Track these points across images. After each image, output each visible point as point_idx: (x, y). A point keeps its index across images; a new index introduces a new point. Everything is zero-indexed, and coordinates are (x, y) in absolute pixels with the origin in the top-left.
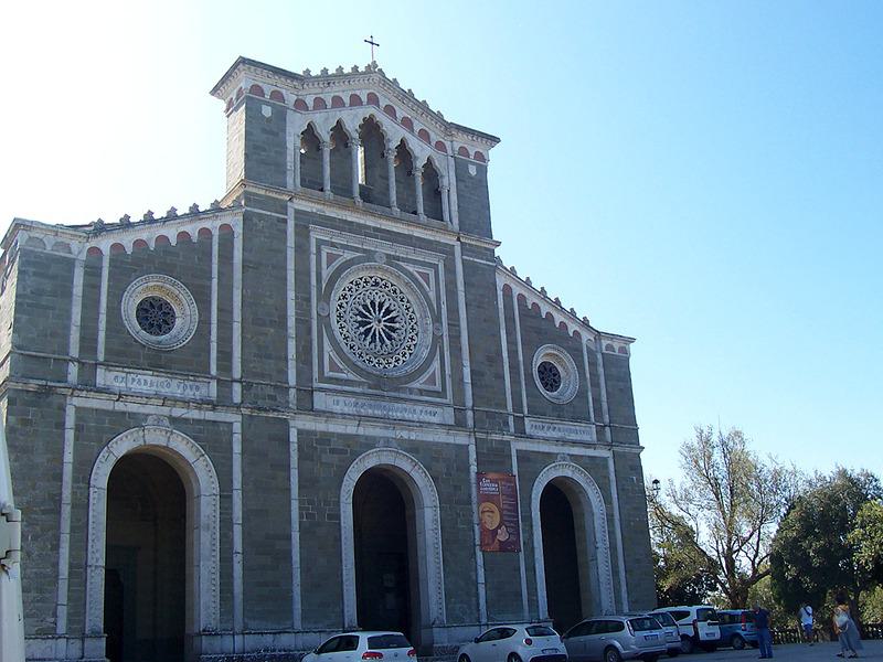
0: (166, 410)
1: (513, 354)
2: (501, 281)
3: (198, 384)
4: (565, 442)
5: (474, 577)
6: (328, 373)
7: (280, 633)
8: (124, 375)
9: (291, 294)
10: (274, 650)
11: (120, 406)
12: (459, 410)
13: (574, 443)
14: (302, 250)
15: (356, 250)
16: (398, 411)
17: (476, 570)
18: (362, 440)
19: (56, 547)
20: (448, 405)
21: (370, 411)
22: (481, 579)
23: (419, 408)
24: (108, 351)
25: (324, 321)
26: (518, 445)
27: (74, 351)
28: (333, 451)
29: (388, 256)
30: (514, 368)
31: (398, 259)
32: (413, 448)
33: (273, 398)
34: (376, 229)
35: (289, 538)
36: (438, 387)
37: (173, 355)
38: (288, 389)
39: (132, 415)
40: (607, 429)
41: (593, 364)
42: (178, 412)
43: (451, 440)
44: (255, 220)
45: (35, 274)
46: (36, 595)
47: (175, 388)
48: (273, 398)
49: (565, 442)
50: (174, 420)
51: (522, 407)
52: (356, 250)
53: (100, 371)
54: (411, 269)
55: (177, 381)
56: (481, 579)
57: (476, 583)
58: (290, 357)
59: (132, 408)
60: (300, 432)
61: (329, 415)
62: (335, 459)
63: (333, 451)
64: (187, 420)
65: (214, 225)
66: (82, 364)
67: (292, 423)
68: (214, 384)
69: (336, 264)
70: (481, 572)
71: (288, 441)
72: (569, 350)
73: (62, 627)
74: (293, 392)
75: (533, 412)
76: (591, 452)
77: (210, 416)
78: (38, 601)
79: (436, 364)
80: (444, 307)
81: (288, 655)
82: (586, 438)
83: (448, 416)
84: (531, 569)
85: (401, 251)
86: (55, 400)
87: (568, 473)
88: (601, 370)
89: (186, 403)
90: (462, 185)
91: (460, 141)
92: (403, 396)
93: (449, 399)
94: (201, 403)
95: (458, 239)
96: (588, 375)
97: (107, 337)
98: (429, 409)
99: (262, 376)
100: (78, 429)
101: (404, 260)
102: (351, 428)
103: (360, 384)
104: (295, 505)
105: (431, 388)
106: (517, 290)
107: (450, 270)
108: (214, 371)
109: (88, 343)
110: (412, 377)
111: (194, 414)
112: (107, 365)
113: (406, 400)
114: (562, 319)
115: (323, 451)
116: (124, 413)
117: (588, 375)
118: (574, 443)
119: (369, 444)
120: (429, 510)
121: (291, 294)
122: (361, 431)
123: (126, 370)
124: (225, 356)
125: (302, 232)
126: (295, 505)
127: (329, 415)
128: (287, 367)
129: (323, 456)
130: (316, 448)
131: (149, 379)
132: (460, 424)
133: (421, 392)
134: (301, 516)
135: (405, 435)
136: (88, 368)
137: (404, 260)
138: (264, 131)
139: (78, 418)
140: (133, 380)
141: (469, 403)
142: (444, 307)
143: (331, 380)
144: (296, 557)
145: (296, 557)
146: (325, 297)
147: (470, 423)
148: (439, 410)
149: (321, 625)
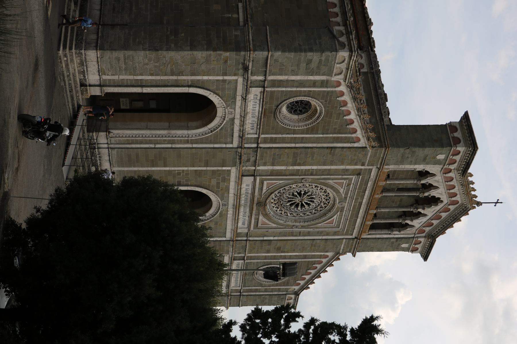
0: (238, 116)
3: (255, 129)
6: (265, 183)
8: (259, 98)
11: (239, 98)
15: (346, 194)
18: (226, 195)
19: (152, 75)
20: (249, 230)
21: (243, 199)
29: (344, 207)
33: (248, 160)
34: (361, 204)
36: (259, 225)
38: (255, 166)
39: (234, 102)
40: (239, 294)
42: (237, 122)
46: (124, 67)
50: (233, 120)
52: (346, 194)
54: (335, 217)
55: (256, 120)
58: (274, 167)
59: (239, 103)
60: (229, 171)
61: (239, 183)
63: (218, 184)
64: (233, 125)
66: (265, 80)
69: (336, 186)
71: (223, 166)
73: (104, 77)
74: (254, 168)
78: (120, 68)
89: (243, 124)
90: (394, 240)
92: (254, 212)
95: (356, 238)
107: (335, 234)
111: (236, 128)
113: (251, 214)
116: (235, 99)
123: (262, 100)
127: (239, 183)
128: (268, 166)
130: (220, 177)
131: (257, 109)
133: (257, 220)
136: (262, 85)
137: (341, 215)
139: (230, 81)
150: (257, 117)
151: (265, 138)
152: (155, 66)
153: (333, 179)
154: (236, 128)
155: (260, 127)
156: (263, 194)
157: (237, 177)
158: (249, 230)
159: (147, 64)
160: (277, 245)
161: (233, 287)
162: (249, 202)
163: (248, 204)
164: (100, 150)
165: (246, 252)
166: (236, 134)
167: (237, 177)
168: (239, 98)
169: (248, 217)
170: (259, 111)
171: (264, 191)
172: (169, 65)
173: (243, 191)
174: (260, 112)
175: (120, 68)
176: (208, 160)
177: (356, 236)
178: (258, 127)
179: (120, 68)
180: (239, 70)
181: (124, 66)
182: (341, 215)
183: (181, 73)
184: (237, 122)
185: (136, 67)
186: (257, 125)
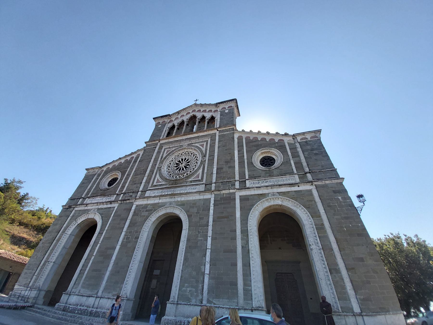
1: (241, 157)
2: (236, 136)
5: (203, 271)
9: (151, 165)
12: (208, 185)
15: (178, 146)
16: (178, 191)
17: (205, 266)
18: (160, 205)
20: (203, 184)
22: (207, 271)
23: (189, 188)
25: (159, 169)
26: (238, 194)
30: (241, 163)
31: (192, 144)
32: (182, 205)
36: (200, 178)
37: (108, 190)
41: (293, 148)
43: (202, 197)
47: (105, 199)
48: (131, 196)
49: (272, 186)
51: (245, 176)
54: (196, 145)
56: (207, 271)
57: (203, 274)
60: (137, 206)
62: (146, 214)
63: (146, 211)
65: (135, 156)
70: (208, 266)
72: (276, 147)
75: (251, 177)
76: (296, 188)
77: (109, 206)
79: (201, 171)
80: (208, 152)
83: (202, 188)
84: (247, 265)
85: (193, 141)
87: (279, 202)
88: (299, 149)
91: (222, 106)
92: (182, 185)
93: (204, 181)
94: (107, 202)
95: (218, 130)
96: (290, 153)
98: (193, 187)
101: (194, 143)
102: (157, 201)
103: (166, 184)
104: (123, 234)
105: (198, 179)
106: (244, 136)
109: (88, 193)
110: (188, 177)
111: (105, 206)
113: (183, 186)
114: (271, 138)
115: (143, 211)
117: (290, 153)
118: (280, 185)
119: (162, 205)
120: (185, 231)
121: (151, 165)
122: (161, 201)
123: (93, 197)
124: (123, 187)
125: (161, 148)
126: (123, 234)
132: (208, 190)
133: (191, 182)
135: (179, 199)
137: (194, 143)
138: (158, 130)
141: (214, 181)
142: (208, 152)
143: (155, 186)
144: (114, 258)
145: (114, 258)
146: (162, 162)
147: (213, 188)
148: (197, 187)
150: (103, 198)
151: (120, 191)
153: (163, 155)
155: (110, 195)
156: (165, 183)
157: (143, 200)
158: (203, 184)
160: (223, 164)
162: (171, 189)
163: (173, 189)
165: (230, 181)
166: (109, 206)
167: (143, 200)
169: (187, 188)
171: (163, 183)
173: (160, 194)
174: (100, 197)
178: (109, 196)
182: (196, 143)
186: (109, 196)
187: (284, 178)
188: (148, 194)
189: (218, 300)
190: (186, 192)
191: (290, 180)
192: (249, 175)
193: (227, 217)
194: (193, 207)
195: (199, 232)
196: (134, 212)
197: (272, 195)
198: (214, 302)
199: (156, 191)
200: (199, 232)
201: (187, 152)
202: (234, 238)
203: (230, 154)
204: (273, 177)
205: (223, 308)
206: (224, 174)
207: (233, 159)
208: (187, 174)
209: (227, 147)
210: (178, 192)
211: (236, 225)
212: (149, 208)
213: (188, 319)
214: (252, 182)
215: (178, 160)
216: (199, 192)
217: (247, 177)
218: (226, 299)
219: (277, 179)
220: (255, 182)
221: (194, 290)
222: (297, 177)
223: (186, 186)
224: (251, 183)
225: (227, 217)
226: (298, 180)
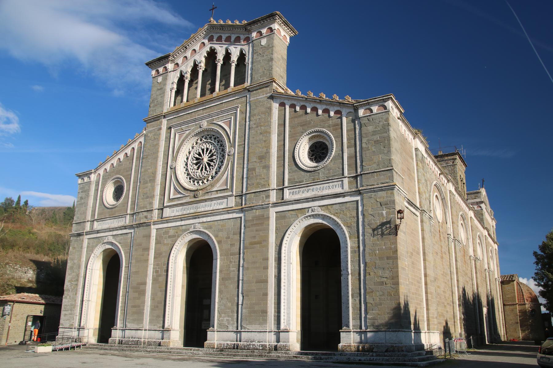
0: (111, 233)
4: (314, 199)
7: (137, 330)
10: (135, 338)
11: (99, 235)
13: (323, 197)
14: (168, 139)
16: (203, 207)
24: (99, 214)
27: (89, 218)
28: (170, 237)
33: (146, 217)
35: (145, 284)
37: (116, 209)
44: (149, 134)
45: (82, 192)
47: (116, 223)
48: (146, 217)
49: (314, 199)
53: (95, 223)
55: (116, 220)
62: (169, 241)
63: (170, 237)
67: (152, 226)
68: (128, 217)
81: (138, 341)
82: (339, 190)
83: (232, 202)
86: (81, 237)
94: (121, 228)
97: (98, 209)
98: (219, 201)
99: (143, 208)
100: (88, 247)
108: (129, 212)
112: (97, 220)
118: (323, 197)
129: (165, 240)
134: (153, 273)
140: (104, 223)
146: (175, 159)
149: (156, 327)
151: (131, 210)
152: (72, 291)
154: (120, 232)
159: (70, 296)
160: (255, 162)
161: (343, 188)
164: (126, 336)
168: (99, 235)
170: (109, 220)
172: (72, 283)
175: (70, 314)
176: (143, 249)
177: (247, 91)
179: (70, 314)
180: (80, 239)
181: (70, 312)
183: (78, 275)
184: (115, 233)
185: (71, 304)
186: (120, 218)
187: (331, 184)
188: (167, 213)
189: (251, 326)
190: (211, 209)
191: (337, 186)
192: (289, 180)
193: (259, 243)
194: (221, 230)
195: (230, 261)
196: (156, 239)
197: (312, 211)
198: (247, 327)
199: (175, 209)
200: (230, 261)
201: (208, 135)
202: (266, 268)
203: (265, 141)
204: (318, 183)
205: (255, 332)
206: (257, 179)
207: (268, 152)
208: (211, 176)
209: (263, 128)
210: (203, 210)
211: (268, 252)
212: (172, 232)
213: (227, 342)
214: (292, 191)
215: (197, 153)
216: (228, 211)
217: (286, 184)
218: (258, 325)
219: (322, 186)
220: (294, 190)
221: (231, 319)
222: (346, 181)
223: (211, 199)
224: (290, 193)
225: (259, 243)
226: (346, 188)
